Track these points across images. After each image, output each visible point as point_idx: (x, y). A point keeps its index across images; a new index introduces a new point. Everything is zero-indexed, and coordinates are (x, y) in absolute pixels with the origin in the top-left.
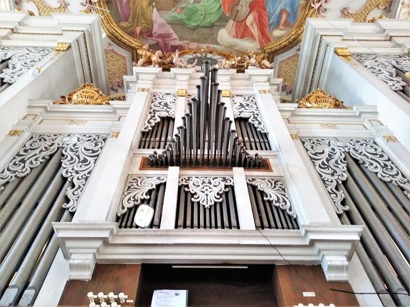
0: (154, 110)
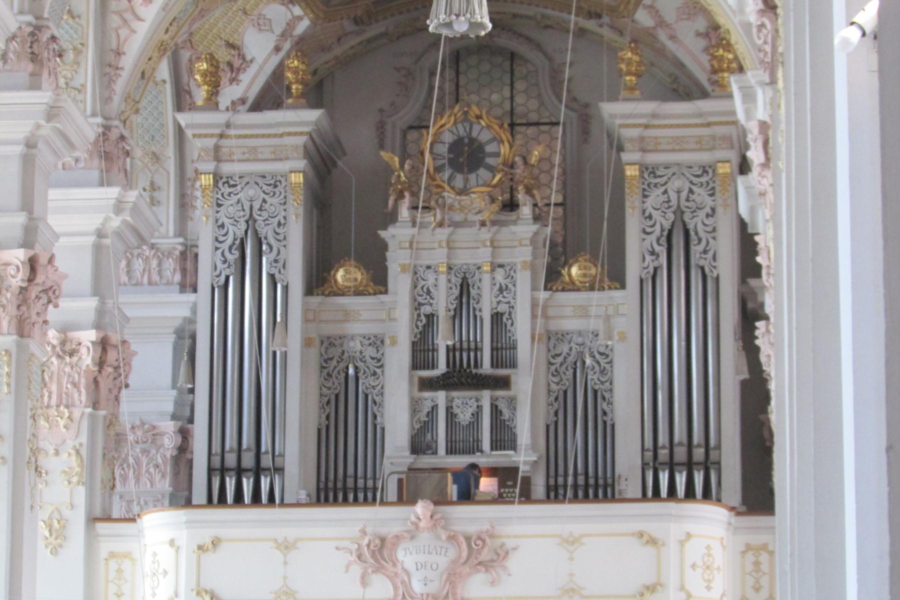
0: (420, 304)
